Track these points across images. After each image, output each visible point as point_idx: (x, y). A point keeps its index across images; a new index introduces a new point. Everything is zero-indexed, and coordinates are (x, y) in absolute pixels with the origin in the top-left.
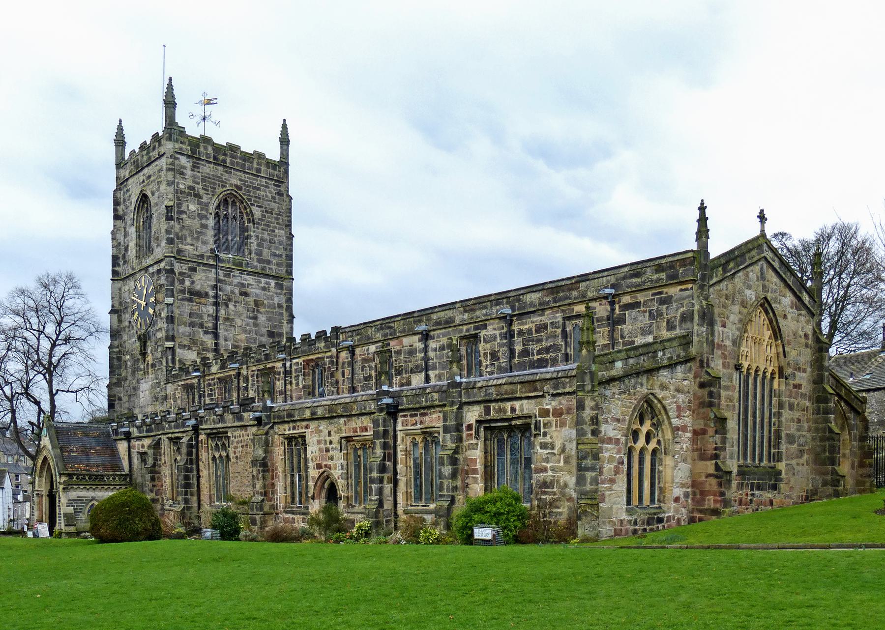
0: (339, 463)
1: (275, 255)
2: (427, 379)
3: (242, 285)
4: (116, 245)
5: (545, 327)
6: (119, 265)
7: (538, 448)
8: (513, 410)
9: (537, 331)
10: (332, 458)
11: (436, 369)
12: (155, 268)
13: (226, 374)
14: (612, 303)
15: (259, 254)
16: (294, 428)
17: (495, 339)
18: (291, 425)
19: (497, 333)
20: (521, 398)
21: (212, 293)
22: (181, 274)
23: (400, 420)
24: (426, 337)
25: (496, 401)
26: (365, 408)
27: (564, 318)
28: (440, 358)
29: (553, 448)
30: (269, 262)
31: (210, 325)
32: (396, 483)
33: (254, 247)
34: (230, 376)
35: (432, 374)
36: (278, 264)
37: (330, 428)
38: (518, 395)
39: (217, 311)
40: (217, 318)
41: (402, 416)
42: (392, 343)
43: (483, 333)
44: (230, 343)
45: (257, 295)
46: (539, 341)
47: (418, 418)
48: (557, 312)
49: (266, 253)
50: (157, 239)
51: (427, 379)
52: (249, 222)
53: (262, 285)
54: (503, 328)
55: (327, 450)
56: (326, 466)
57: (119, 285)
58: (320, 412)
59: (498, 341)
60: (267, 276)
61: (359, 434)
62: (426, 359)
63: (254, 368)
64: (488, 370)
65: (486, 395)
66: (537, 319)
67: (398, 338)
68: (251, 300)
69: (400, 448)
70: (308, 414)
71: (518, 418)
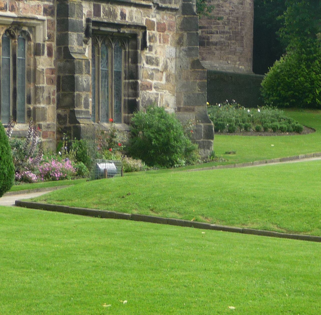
7: (144, 62)
8: (123, 16)
29: (157, 65)
71: (129, 26)
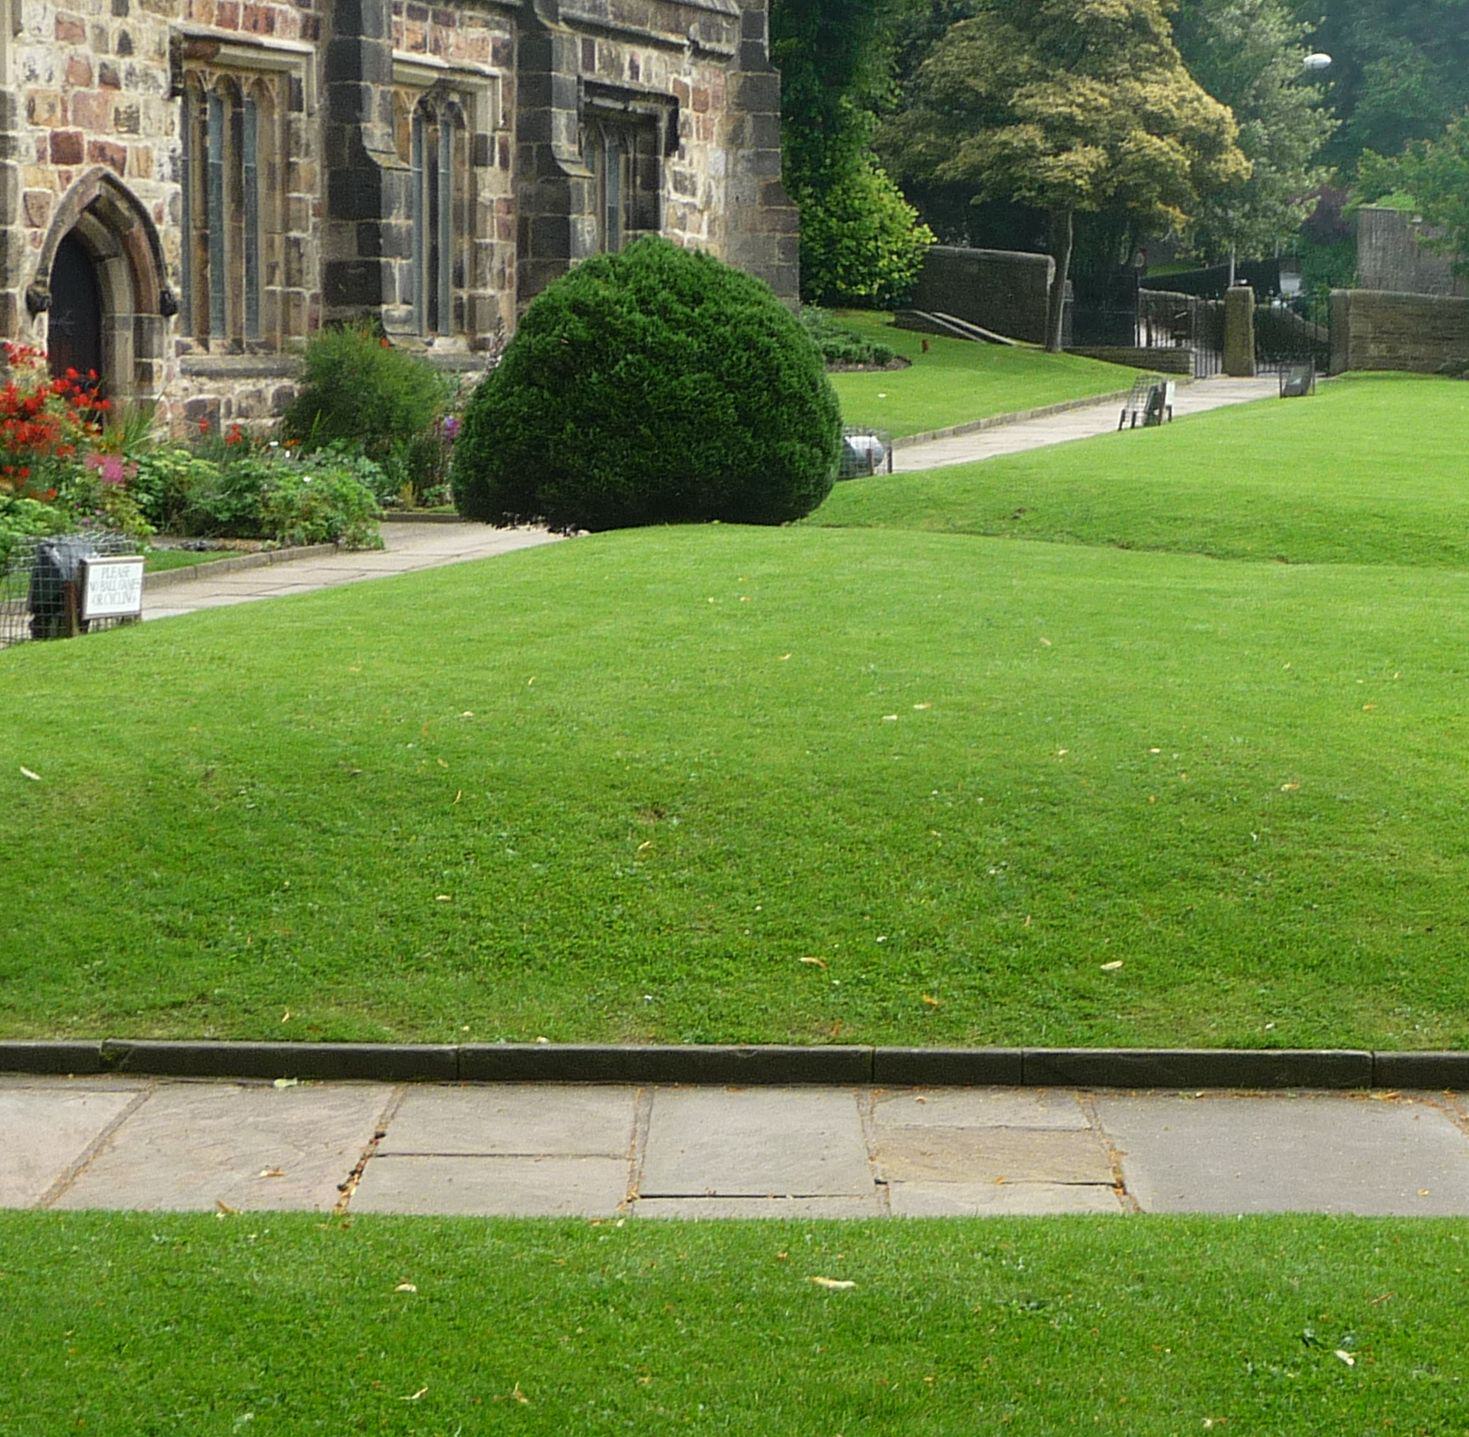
7: (670, 185)
55: (110, 81)
56: (100, 152)
61: (240, 34)
71: (645, 96)
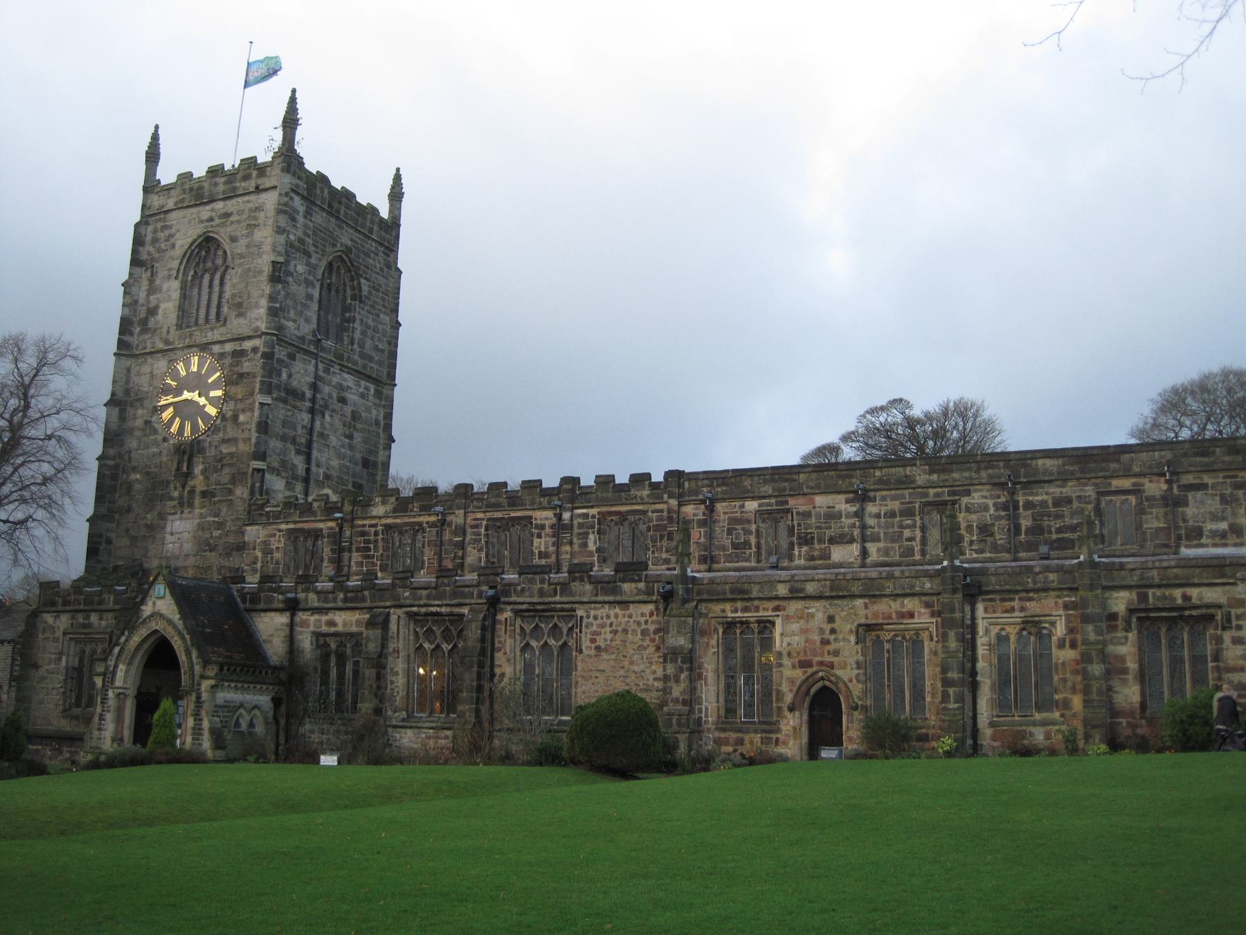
0: (852, 661)
1: (376, 349)
2: (864, 553)
3: (340, 387)
4: (130, 302)
5: (1069, 501)
6: (131, 334)
8: (1186, 598)
9: (1055, 504)
10: (836, 653)
11: (879, 540)
12: (229, 347)
13: (406, 520)
14: (1169, 482)
15: (362, 346)
16: (745, 610)
17: (986, 508)
18: (739, 604)
19: (990, 502)
20: (1199, 585)
21: (309, 394)
22: (280, 361)
23: (980, 607)
24: (863, 497)
25: (1159, 586)
26: (913, 587)
27: (1098, 493)
28: (887, 527)
30: (370, 359)
31: (303, 440)
32: (974, 687)
33: (357, 335)
34: (420, 524)
35: (872, 548)
36: (380, 363)
37: (831, 611)
38: (1196, 581)
39: (313, 421)
40: (311, 431)
41: (984, 600)
42: (792, 502)
43: (965, 500)
44: (321, 471)
45: (355, 404)
46: (1059, 516)
47: (1016, 604)
48: (1086, 485)
49: (368, 343)
50: (240, 305)
51: (864, 553)
52: (354, 298)
53: (361, 390)
54: (999, 497)
55: (825, 642)
56: (821, 663)
57: (127, 363)
58: (810, 588)
59: (992, 511)
60: (369, 378)
62: (864, 527)
63: (480, 515)
64: (975, 547)
65: (1142, 579)
66: (1055, 490)
67: (805, 494)
68: (348, 410)
69: (981, 641)
70: (782, 590)
71: (1196, 607)
